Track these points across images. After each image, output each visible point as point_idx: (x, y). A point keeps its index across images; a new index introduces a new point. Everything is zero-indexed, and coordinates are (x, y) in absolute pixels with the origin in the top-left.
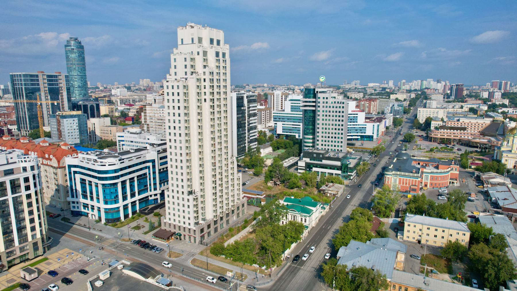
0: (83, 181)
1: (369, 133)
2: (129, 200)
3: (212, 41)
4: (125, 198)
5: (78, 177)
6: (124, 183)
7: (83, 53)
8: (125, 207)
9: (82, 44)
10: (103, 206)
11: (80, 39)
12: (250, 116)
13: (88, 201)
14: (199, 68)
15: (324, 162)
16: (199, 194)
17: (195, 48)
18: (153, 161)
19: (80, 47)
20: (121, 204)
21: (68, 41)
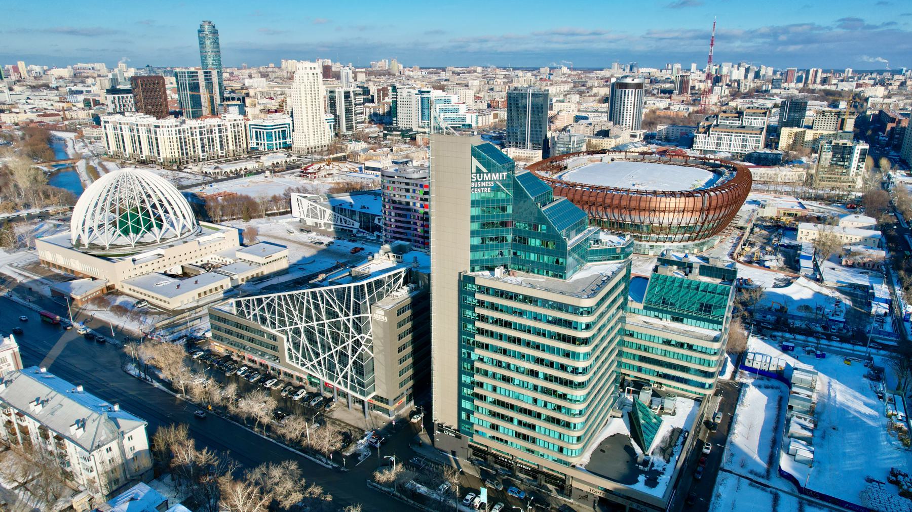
0: (256, 132)
1: (468, 122)
2: (278, 142)
3: (311, 68)
4: (276, 140)
5: (254, 130)
6: (275, 132)
7: (217, 38)
8: (276, 144)
9: (216, 28)
10: (266, 142)
11: (213, 23)
12: (356, 105)
13: (259, 142)
14: (305, 81)
15: (395, 133)
16: (307, 134)
17: (304, 72)
18: (289, 124)
19: (215, 32)
20: (274, 142)
21: (201, 26)
